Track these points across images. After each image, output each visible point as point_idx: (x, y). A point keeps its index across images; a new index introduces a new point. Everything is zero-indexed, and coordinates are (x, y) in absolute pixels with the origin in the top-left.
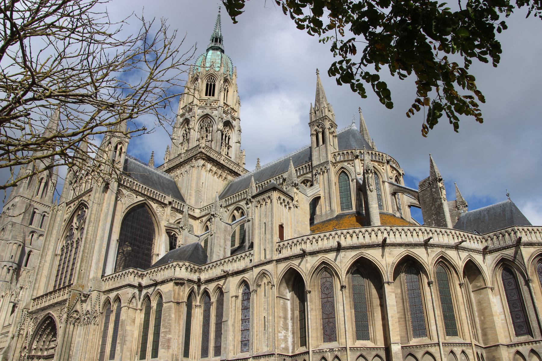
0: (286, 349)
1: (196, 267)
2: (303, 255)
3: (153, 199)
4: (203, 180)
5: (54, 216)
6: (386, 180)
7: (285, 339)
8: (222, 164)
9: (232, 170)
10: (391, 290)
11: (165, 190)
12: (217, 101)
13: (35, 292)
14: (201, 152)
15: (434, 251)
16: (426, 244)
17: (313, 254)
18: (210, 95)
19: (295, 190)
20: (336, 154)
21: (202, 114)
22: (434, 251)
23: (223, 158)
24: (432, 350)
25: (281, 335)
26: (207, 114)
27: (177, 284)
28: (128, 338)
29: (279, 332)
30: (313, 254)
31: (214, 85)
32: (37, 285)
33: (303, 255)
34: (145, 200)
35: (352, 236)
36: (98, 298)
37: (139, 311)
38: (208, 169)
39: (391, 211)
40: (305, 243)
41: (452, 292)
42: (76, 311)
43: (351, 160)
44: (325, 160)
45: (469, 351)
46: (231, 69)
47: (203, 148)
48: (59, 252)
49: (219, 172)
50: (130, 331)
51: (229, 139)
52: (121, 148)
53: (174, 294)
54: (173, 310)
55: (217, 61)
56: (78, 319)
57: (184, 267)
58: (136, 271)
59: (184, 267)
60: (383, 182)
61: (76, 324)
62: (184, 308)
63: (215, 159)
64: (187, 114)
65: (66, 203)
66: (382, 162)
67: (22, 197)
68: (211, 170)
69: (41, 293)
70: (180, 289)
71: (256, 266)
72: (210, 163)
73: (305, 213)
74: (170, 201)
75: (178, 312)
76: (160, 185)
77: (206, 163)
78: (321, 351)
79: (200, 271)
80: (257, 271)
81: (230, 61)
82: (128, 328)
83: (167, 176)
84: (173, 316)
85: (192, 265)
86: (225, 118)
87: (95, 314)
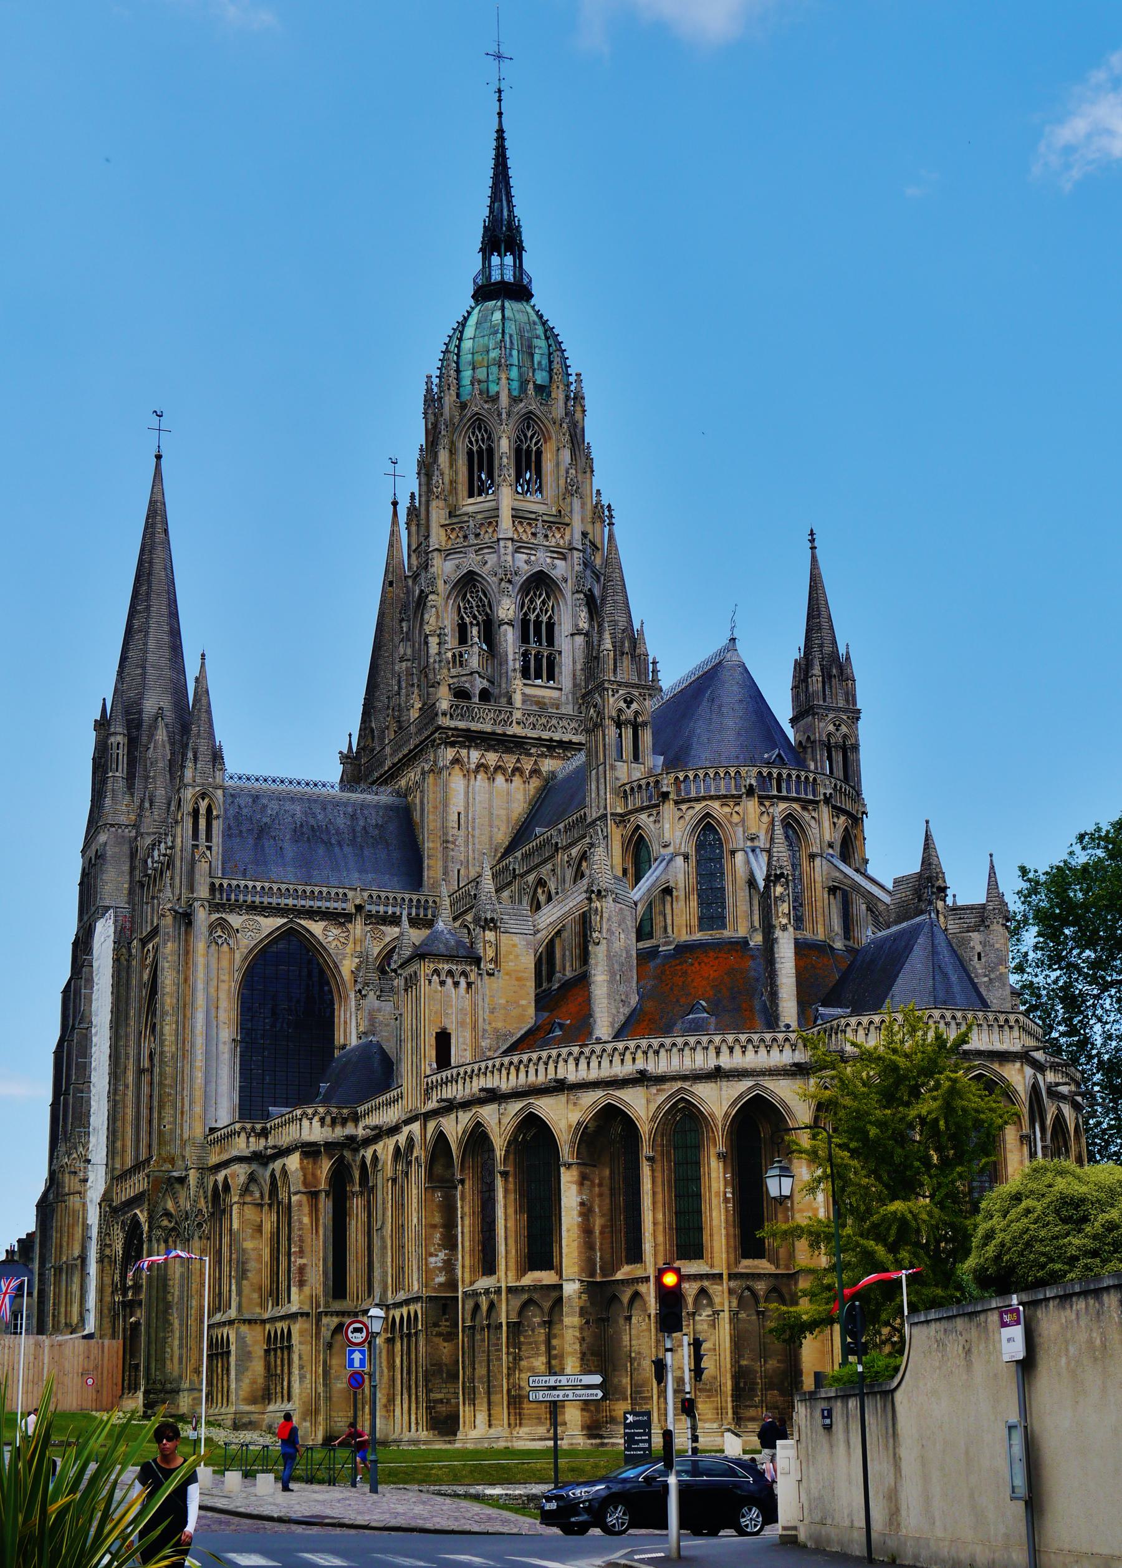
0: (452, 1284)
1: (345, 1111)
2: (450, 1107)
3: (311, 914)
4: (457, 803)
5: (124, 974)
6: (741, 846)
7: (449, 1266)
8: (514, 736)
9: (551, 740)
10: (569, 1179)
11: (366, 853)
12: (492, 518)
13: (118, 1160)
14: (439, 728)
15: (664, 1090)
16: (642, 1079)
17: (466, 1105)
18: (480, 495)
19: (490, 935)
20: (627, 788)
21: (455, 577)
22: (664, 1090)
23: (517, 715)
24: (642, 1288)
25: (436, 1261)
26: (471, 573)
27: (305, 1155)
28: (252, 1265)
29: (431, 1255)
30: (466, 1105)
31: (490, 451)
32: (119, 1144)
33: (450, 1107)
34: (291, 921)
35: (518, 1070)
36: (201, 1184)
37: (266, 1208)
38: (473, 766)
39: (742, 932)
40: (457, 1082)
41: (704, 1170)
42: (168, 1214)
43: (657, 806)
44: (602, 811)
45: (715, 1289)
46: (545, 362)
47: (444, 714)
48: (146, 1064)
49: (510, 761)
50: (254, 1249)
51: (551, 626)
52: (209, 810)
53: (305, 1176)
54: (306, 1209)
55: (494, 354)
56: (173, 1229)
57: (316, 1118)
58: (249, 1126)
59: (316, 1118)
60: (733, 853)
61: (170, 1240)
62: (325, 1205)
63: (488, 728)
64: (423, 574)
65: (141, 940)
66: (733, 796)
67: (112, 825)
68: (479, 766)
69: (129, 1164)
70: (315, 1163)
71: (407, 1122)
72: (477, 747)
73: (518, 979)
74: (358, 902)
75: (314, 1210)
76: (353, 842)
77: (464, 752)
78: (475, 1294)
79: (356, 1119)
80: (406, 1130)
81: (540, 330)
82: (248, 1245)
83: (383, 797)
84: (306, 1220)
85: (335, 1110)
86: (526, 567)
87: (200, 1217)
